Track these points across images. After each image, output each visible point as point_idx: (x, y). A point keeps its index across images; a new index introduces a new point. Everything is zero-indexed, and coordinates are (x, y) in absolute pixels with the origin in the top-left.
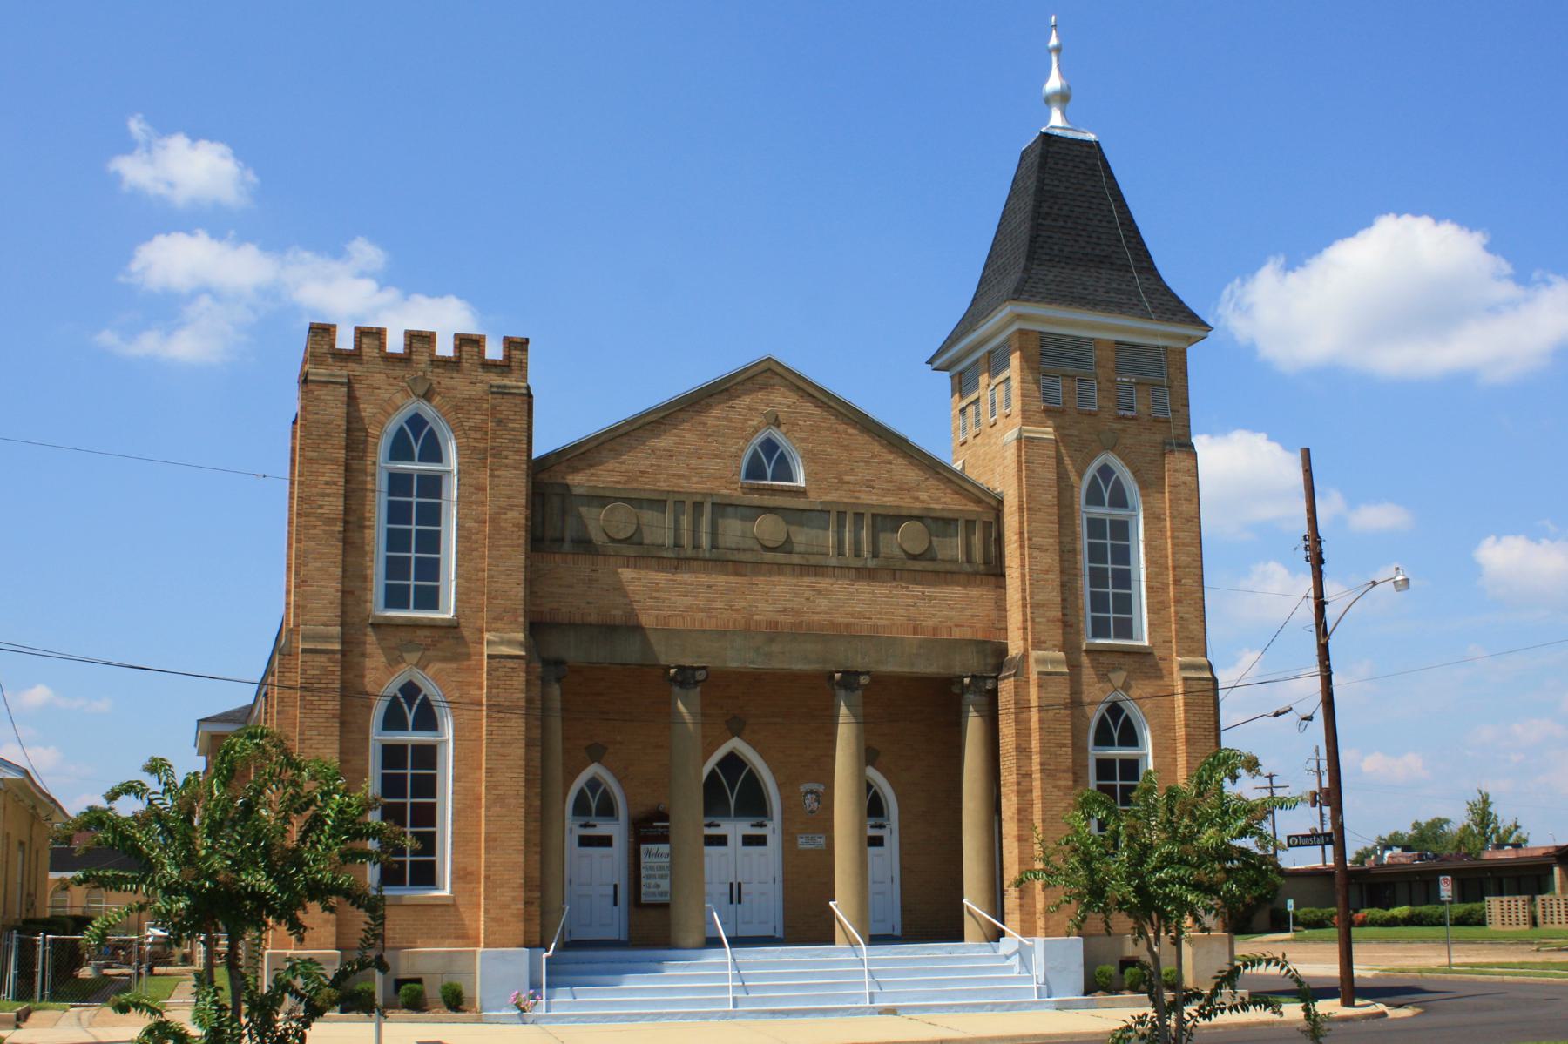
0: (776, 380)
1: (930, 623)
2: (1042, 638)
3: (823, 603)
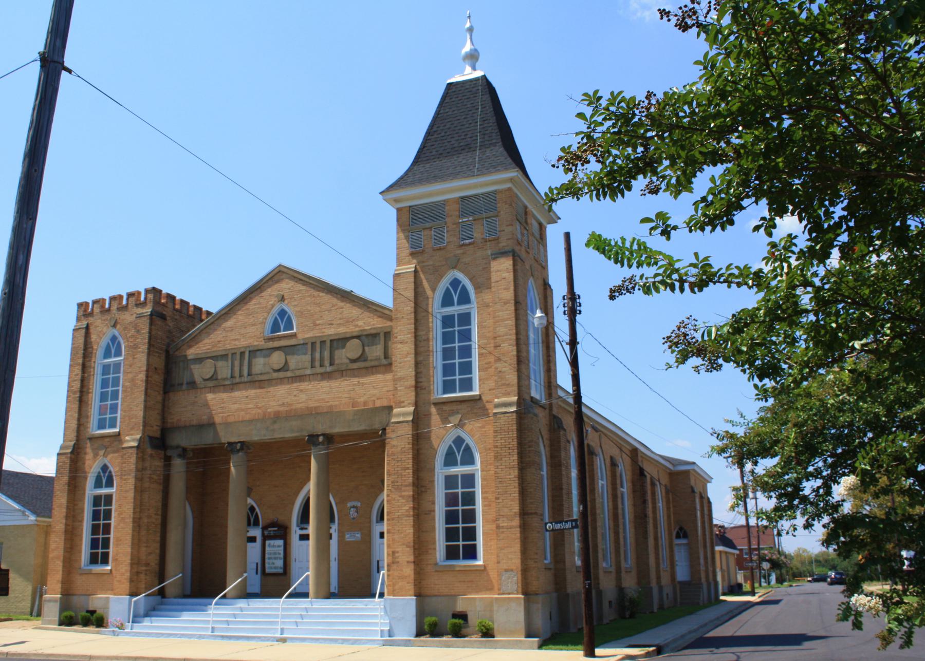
0: (284, 276)
1: (362, 400)
2: (402, 400)
3: (303, 397)
